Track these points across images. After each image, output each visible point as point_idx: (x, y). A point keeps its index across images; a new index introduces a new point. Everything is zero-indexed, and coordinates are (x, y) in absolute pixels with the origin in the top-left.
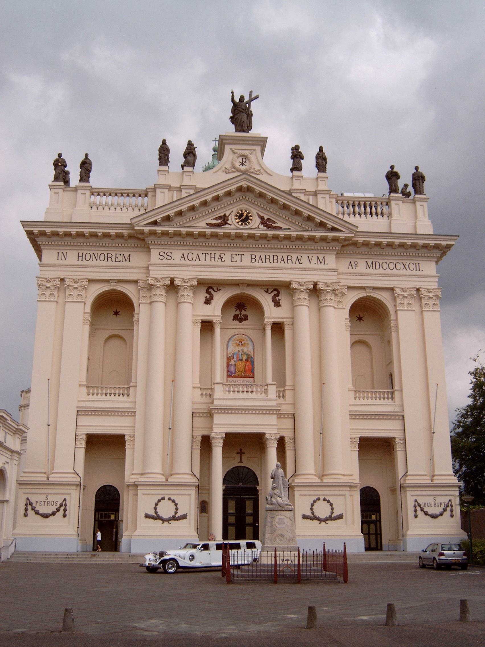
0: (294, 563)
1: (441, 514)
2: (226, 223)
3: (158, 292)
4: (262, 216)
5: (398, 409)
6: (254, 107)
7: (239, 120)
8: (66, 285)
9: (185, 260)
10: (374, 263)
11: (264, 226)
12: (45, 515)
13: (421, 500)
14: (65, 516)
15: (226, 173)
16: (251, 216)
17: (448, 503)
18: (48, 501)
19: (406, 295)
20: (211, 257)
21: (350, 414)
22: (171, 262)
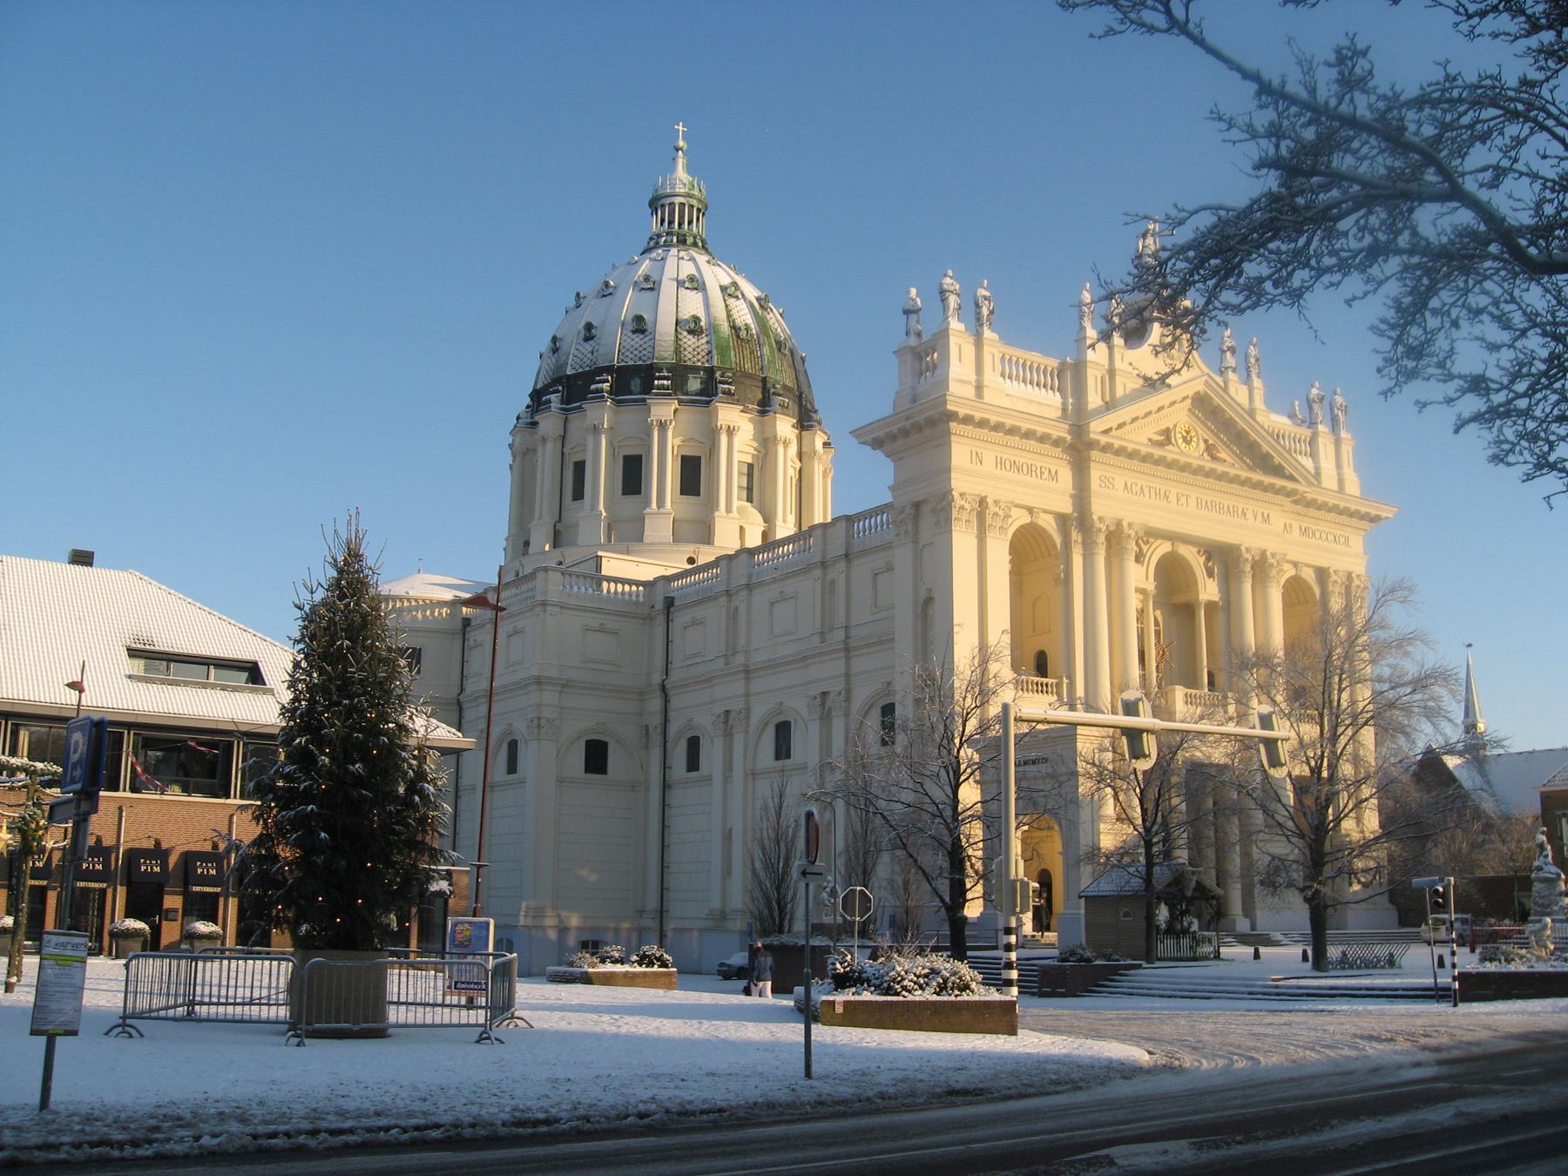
2: (1170, 443)
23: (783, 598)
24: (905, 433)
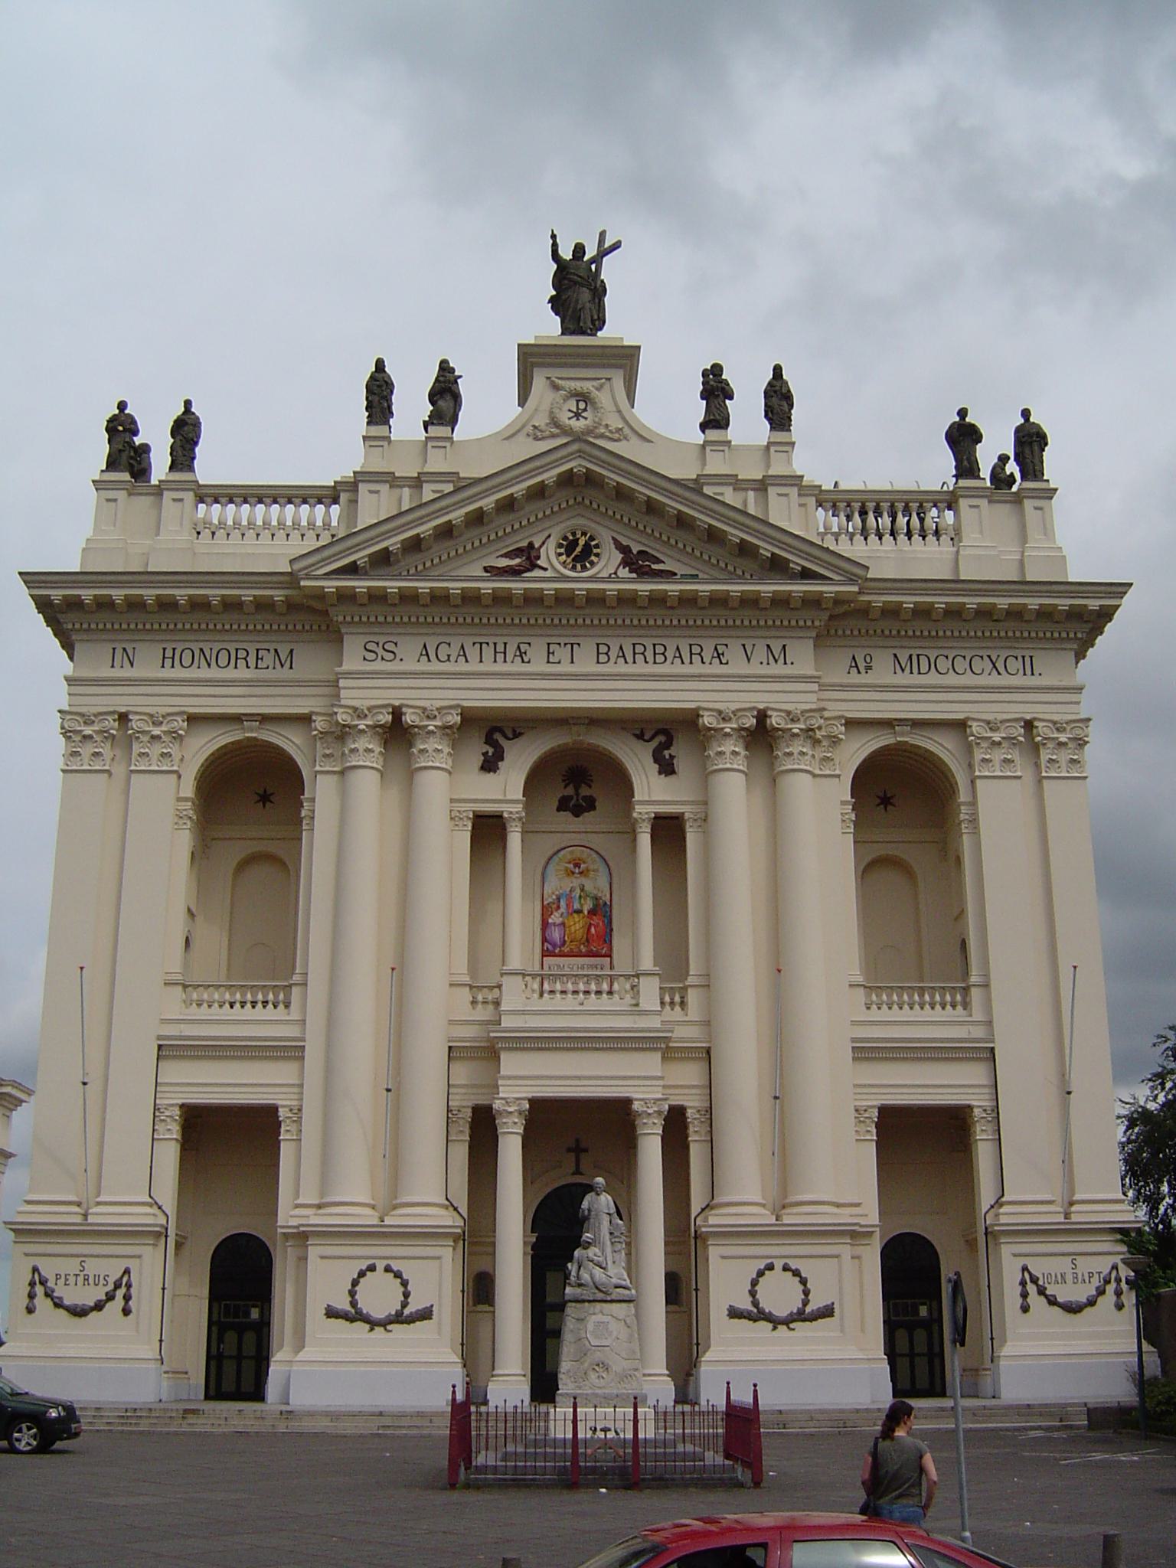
0: (622, 1436)
1: (1091, 1303)
3: (362, 743)
4: (625, 543)
5: (978, 1032)
6: (610, 272)
7: (572, 305)
8: (132, 729)
9: (429, 660)
10: (914, 658)
11: (631, 571)
12: (78, 1310)
13: (1037, 1267)
14: (126, 1312)
15: (536, 439)
16: (597, 546)
17: (1110, 1273)
18: (85, 1275)
19: (997, 739)
20: (495, 652)
21: (853, 1048)
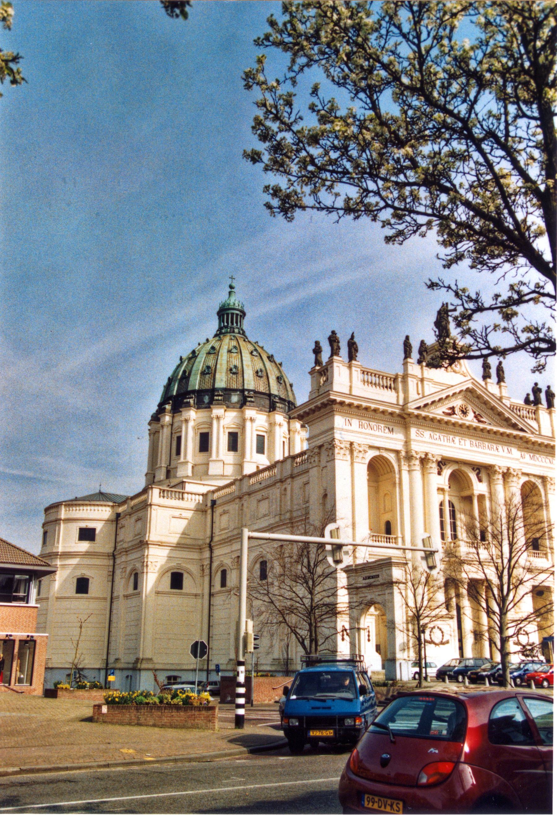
2: (454, 413)
22: (423, 439)
23: (264, 499)
24: (313, 411)
